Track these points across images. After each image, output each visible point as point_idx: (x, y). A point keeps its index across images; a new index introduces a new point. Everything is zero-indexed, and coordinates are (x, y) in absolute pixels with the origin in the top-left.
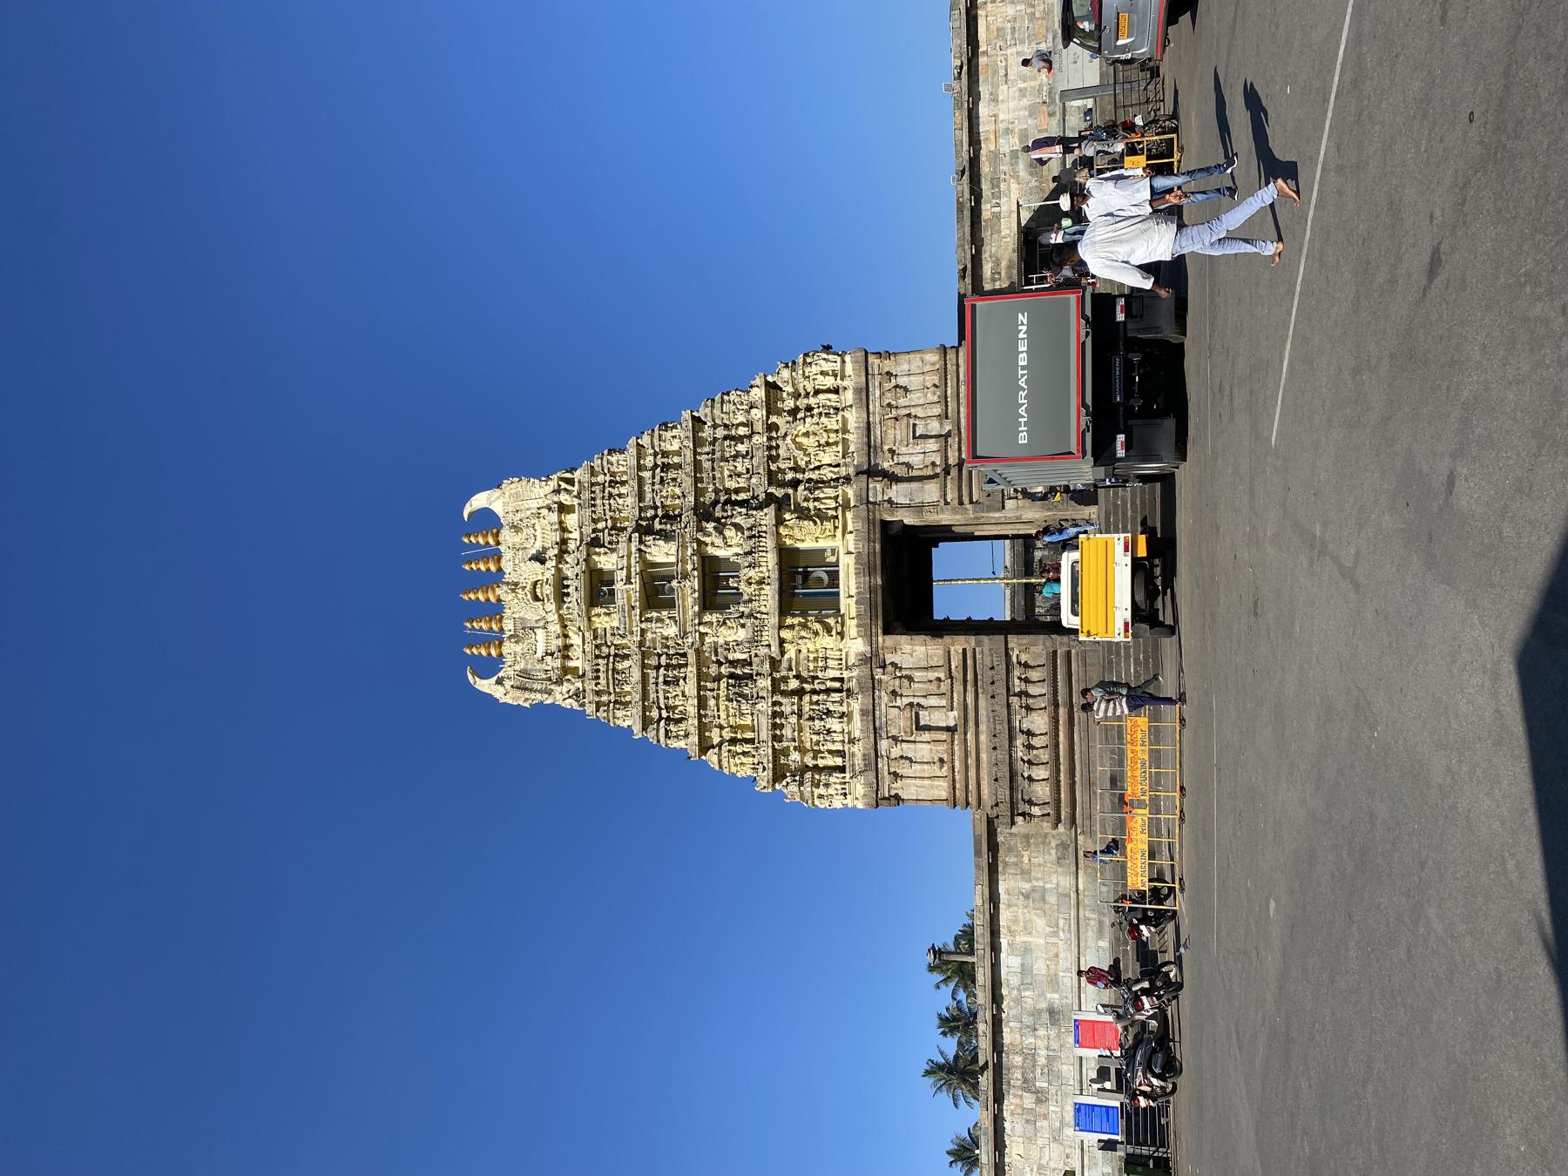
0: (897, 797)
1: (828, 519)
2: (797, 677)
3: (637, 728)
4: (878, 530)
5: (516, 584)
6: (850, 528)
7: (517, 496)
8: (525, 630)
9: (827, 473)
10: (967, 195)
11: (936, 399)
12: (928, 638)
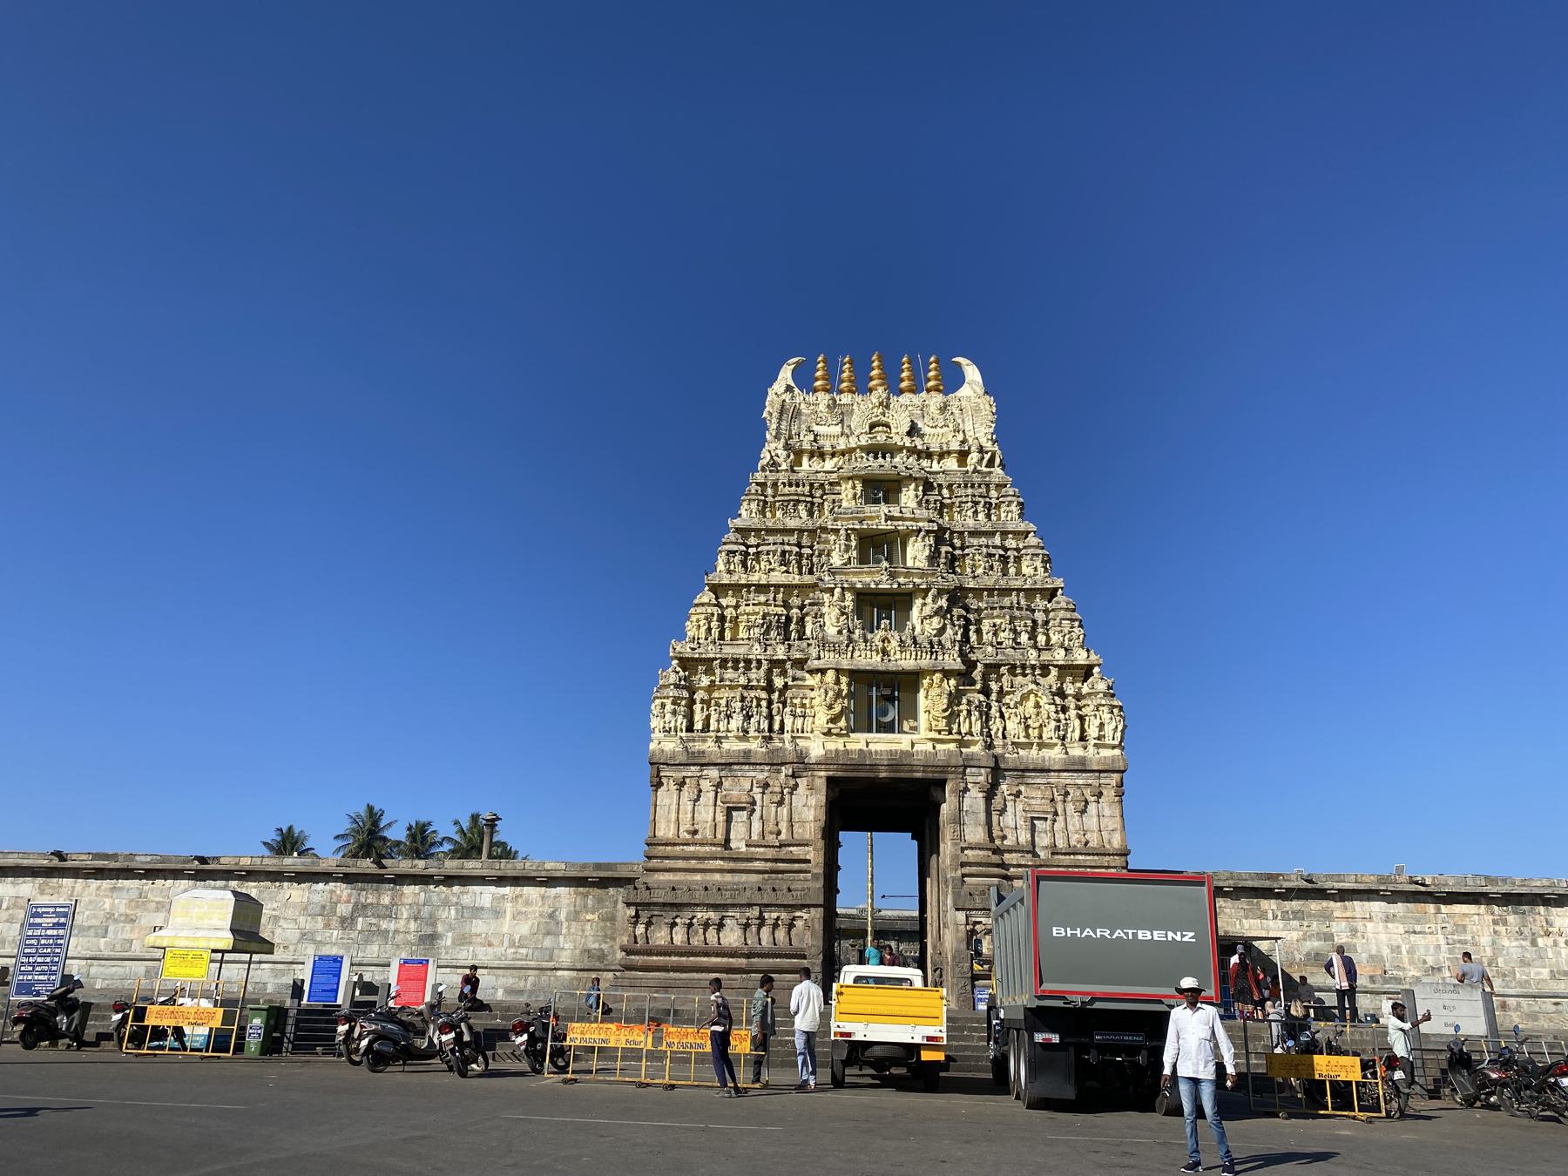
0: (660, 784)
1: (948, 724)
2: (786, 686)
3: (738, 522)
5: (887, 407)
6: (939, 747)
7: (977, 410)
8: (841, 415)
9: (996, 725)
10: (1286, 885)
11: (1073, 843)
12: (822, 824)
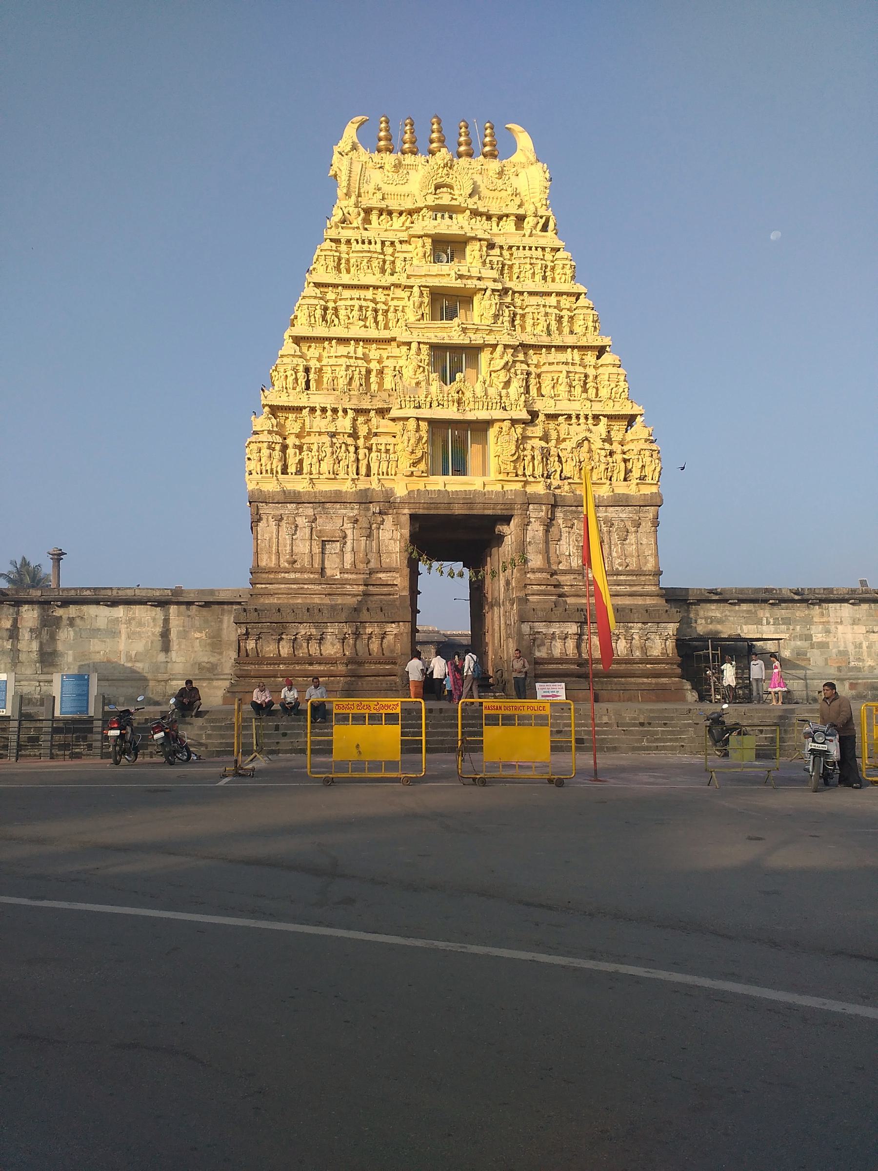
1: (515, 468)
4: (505, 513)
